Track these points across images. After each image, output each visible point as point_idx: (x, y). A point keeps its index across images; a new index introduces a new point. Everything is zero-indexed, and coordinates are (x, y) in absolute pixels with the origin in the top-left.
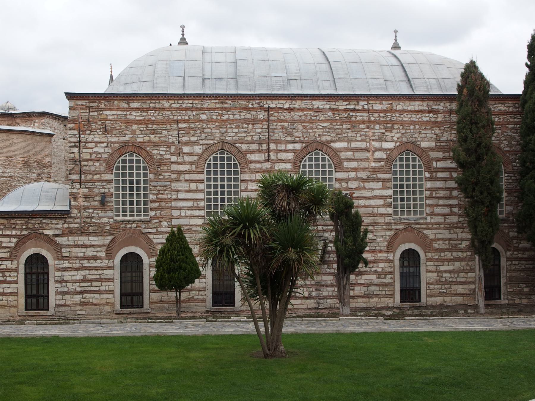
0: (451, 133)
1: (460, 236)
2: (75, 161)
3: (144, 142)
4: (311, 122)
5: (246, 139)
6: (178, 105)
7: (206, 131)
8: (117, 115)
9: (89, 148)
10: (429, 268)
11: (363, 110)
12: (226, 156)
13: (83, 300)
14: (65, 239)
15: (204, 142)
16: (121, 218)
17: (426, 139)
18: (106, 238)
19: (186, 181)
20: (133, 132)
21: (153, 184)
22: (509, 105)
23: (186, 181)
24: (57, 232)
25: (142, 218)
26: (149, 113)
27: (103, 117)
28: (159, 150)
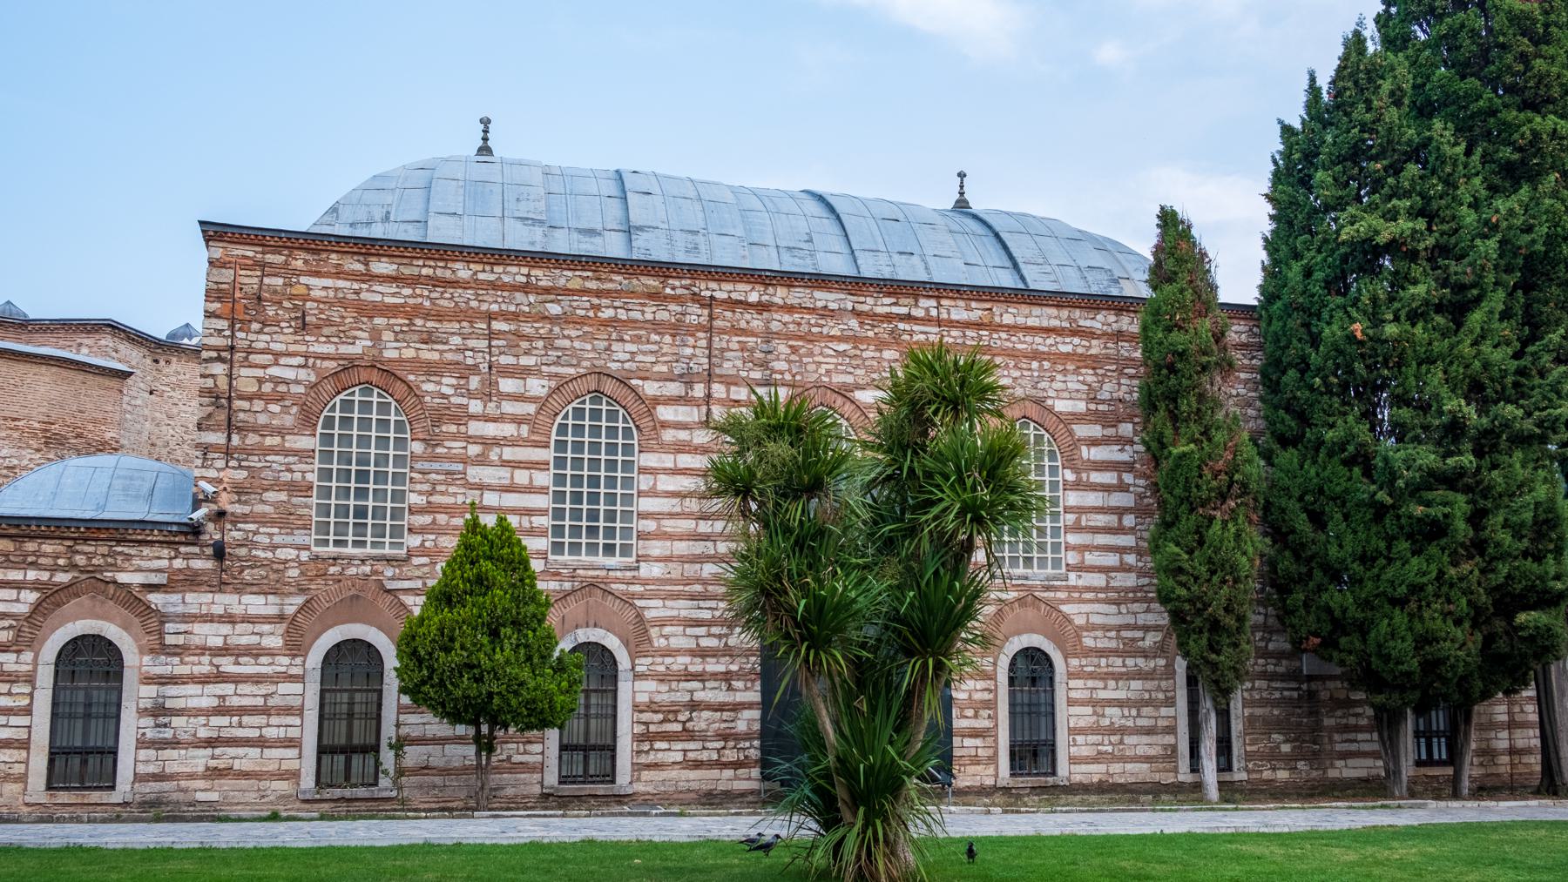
0: (1119, 384)
1: (1142, 619)
2: (217, 398)
3: (400, 361)
4: (809, 338)
5: (656, 369)
6: (492, 277)
7: (558, 343)
8: (337, 289)
9: (256, 366)
10: (1073, 694)
11: (927, 320)
12: (604, 407)
13: (212, 763)
14: (176, 598)
15: (554, 369)
16: (331, 549)
17: (1066, 395)
18: (287, 601)
19: (505, 463)
20: (376, 335)
21: (418, 466)
22: (1242, 328)
23: (505, 463)
24: (154, 579)
25: (387, 551)
26: (418, 291)
27: (300, 290)
28: (440, 383)
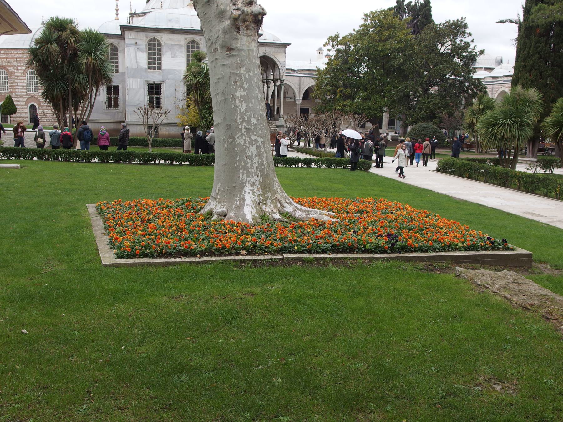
20: (2, 62)
